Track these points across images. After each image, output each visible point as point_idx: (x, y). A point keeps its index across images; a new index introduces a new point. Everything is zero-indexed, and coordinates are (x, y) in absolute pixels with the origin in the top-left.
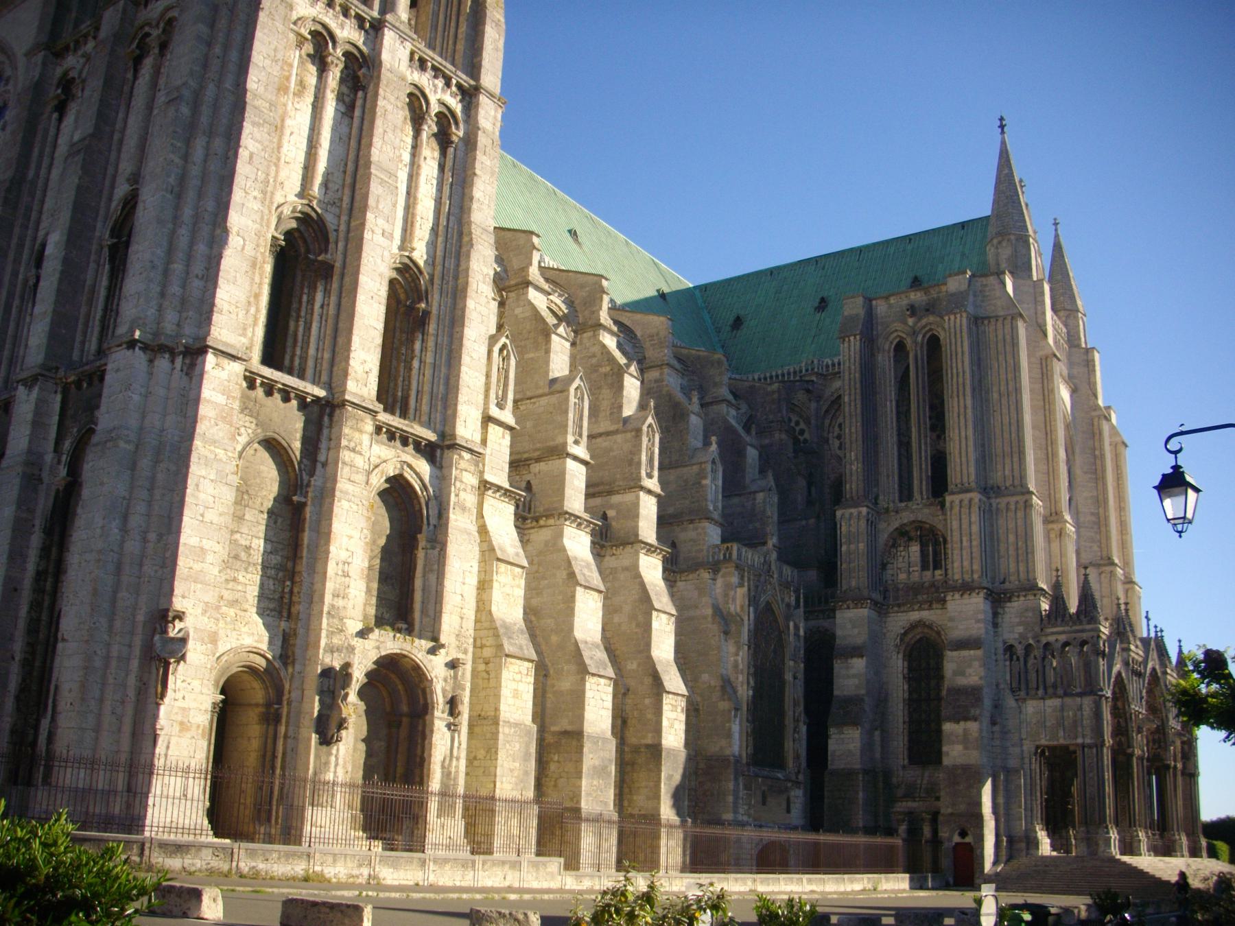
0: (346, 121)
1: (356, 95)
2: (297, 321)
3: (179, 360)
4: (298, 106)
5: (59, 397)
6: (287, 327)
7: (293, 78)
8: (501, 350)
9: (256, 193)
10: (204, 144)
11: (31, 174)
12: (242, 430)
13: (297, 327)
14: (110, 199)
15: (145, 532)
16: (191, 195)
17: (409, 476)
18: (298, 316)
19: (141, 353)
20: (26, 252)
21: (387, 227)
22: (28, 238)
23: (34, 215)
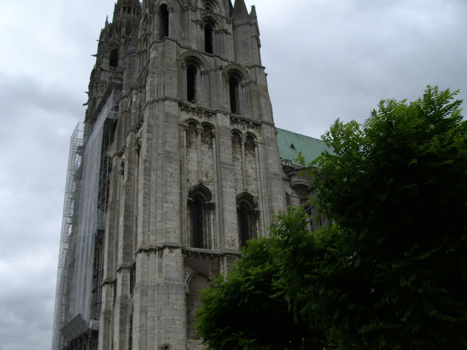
0: (210, 150)
2: (206, 227)
3: (157, 253)
4: (190, 151)
5: (129, 274)
6: (202, 231)
11: (118, 198)
12: (187, 273)
13: (206, 230)
15: (154, 317)
18: (206, 226)
19: (144, 253)
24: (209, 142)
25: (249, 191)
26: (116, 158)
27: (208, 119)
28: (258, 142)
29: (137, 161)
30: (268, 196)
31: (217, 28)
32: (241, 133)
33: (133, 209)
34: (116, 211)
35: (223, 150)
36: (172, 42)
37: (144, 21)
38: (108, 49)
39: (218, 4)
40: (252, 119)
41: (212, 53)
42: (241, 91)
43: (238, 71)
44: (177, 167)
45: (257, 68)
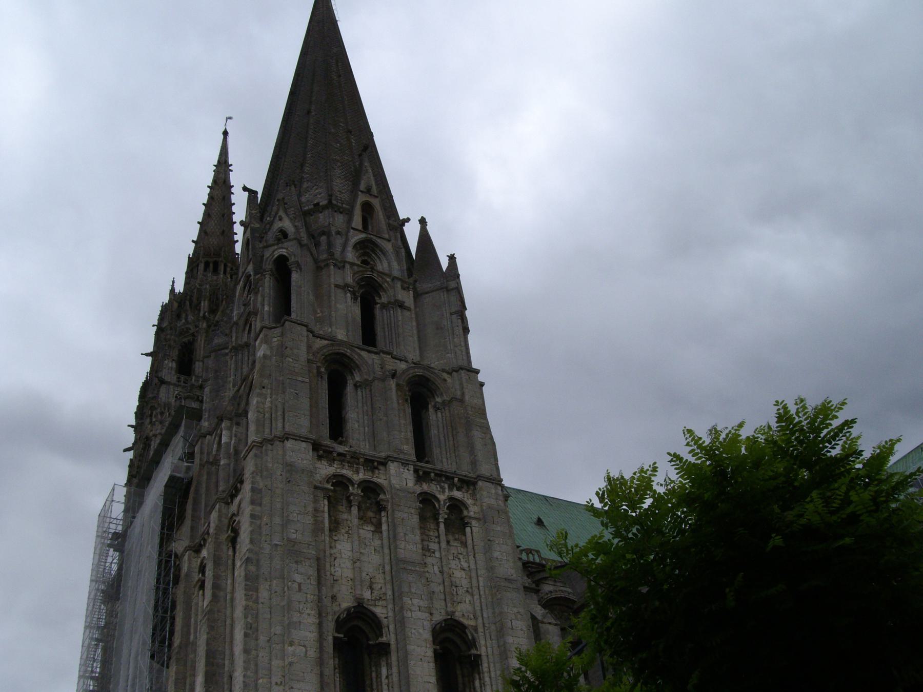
0: (377, 535)
11: (192, 637)
24: (374, 520)
25: (458, 616)
27: (370, 473)
28: (471, 518)
29: (230, 562)
30: (495, 624)
31: (384, 299)
32: (438, 500)
33: (224, 659)
34: (189, 664)
35: (402, 534)
36: (299, 328)
37: (245, 288)
38: (175, 341)
39: (384, 254)
40: (458, 472)
41: (375, 346)
42: (434, 418)
43: (428, 380)
44: (312, 572)
45: (462, 372)
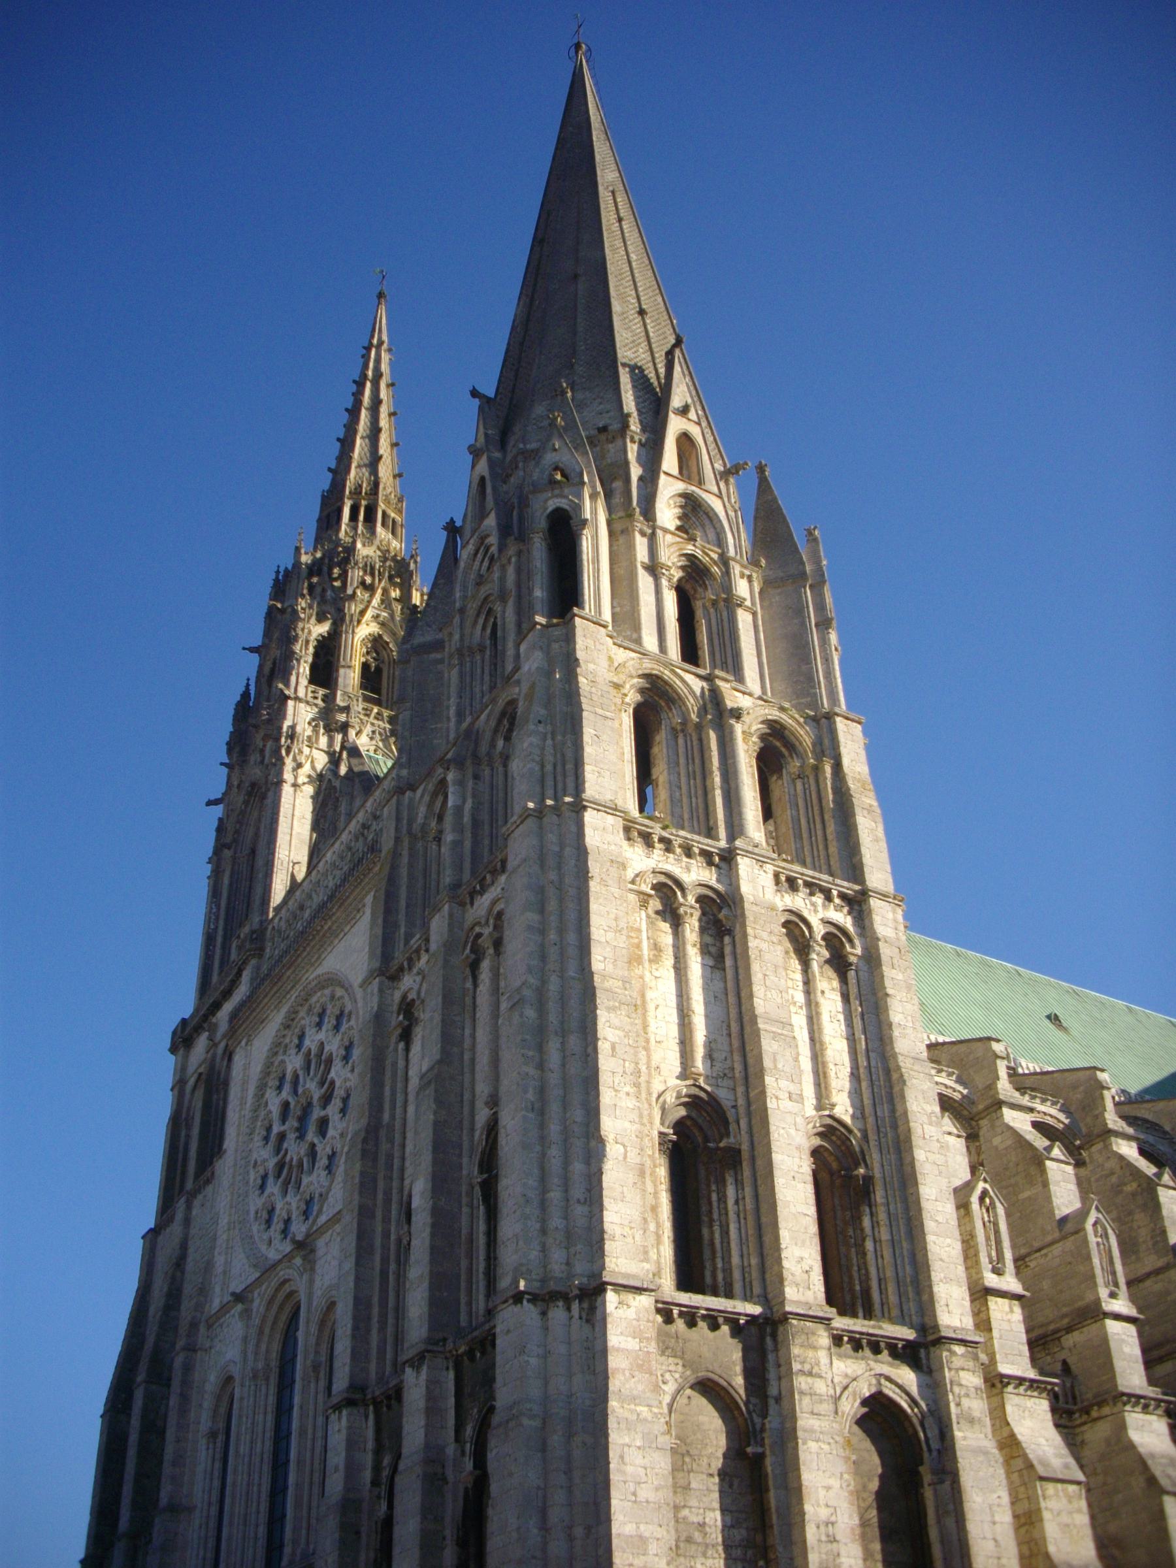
0: (718, 974)
1: (722, 941)
2: (711, 1226)
3: (575, 1306)
4: (657, 974)
5: (451, 1374)
7: (645, 944)
8: (982, 1199)
9: (628, 1089)
10: (558, 1045)
11: (386, 1116)
13: (712, 1233)
14: (472, 1130)
15: (570, 1527)
16: (554, 1108)
17: (890, 1391)
18: (711, 1220)
19: (531, 1306)
20: (394, 1206)
21: (792, 1088)
22: (395, 1191)
23: (396, 1162)
26: (381, 983)
29: (468, 1000)
33: (460, 1156)
34: (382, 1159)
35: (760, 976)
41: (697, 665)
